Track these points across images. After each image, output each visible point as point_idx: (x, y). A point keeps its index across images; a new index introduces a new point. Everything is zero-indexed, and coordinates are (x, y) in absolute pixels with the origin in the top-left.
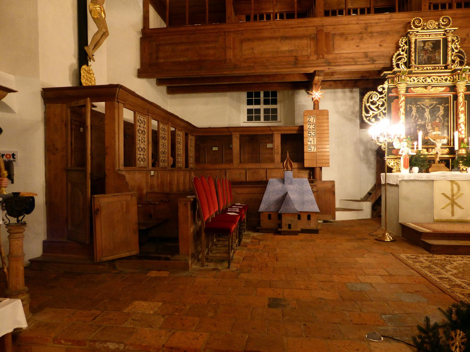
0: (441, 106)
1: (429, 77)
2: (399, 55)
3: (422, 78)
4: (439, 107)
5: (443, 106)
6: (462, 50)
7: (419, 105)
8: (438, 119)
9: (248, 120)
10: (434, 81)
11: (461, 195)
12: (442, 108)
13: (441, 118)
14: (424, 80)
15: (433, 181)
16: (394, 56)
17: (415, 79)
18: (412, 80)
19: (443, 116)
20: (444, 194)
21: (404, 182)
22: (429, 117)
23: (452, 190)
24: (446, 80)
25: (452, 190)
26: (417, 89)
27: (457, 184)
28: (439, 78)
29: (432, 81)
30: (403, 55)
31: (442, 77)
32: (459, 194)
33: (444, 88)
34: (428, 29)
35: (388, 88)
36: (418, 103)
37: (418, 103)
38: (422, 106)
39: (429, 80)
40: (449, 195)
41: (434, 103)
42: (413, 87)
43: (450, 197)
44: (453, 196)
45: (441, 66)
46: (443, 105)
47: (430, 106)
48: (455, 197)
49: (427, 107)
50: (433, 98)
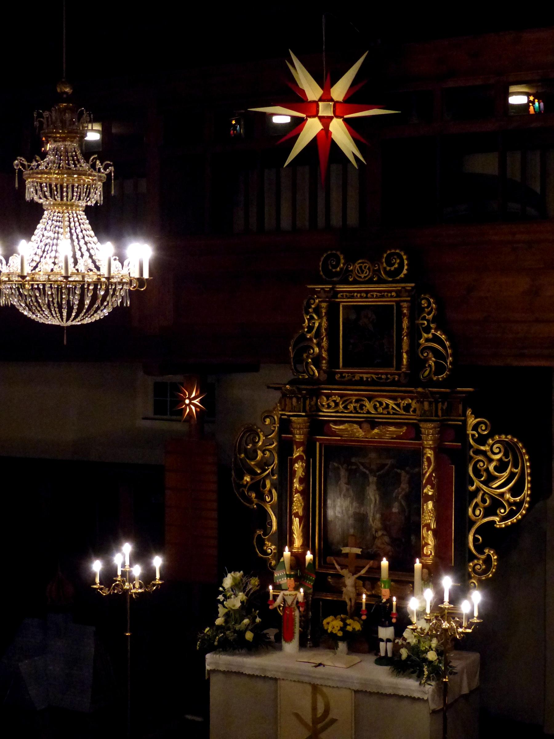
0: (403, 473)
1: (370, 398)
2: (303, 337)
3: (354, 399)
4: (400, 475)
5: (407, 472)
6: (438, 333)
7: (355, 464)
8: (396, 504)
9: (155, 413)
10: (380, 410)
11: (333, 721)
12: (405, 477)
13: (403, 503)
14: (358, 405)
15: (276, 680)
16: (292, 342)
17: (338, 399)
18: (333, 404)
19: (407, 497)
20: (297, 715)
21: (221, 677)
22: (378, 498)
23: (314, 709)
24: (407, 408)
25: (314, 709)
26: (341, 427)
27: (324, 696)
28: (391, 403)
29: (375, 408)
30: (311, 339)
31: (399, 401)
32: (327, 720)
33: (404, 429)
34: (355, 282)
35: (281, 420)
36: (353, 460)
37: (353, 460)
38: (361, 467)
39: (368, 406)
40: (308, 718)
41: (389, 462)
42: (336, 423)
43: (311, 725)
44: (316, 721)
45: (392, 374)
46: (407, 468)
47: (379, 469)
48: (319, 726)
49: (371, 471)
50: (384, 450)
